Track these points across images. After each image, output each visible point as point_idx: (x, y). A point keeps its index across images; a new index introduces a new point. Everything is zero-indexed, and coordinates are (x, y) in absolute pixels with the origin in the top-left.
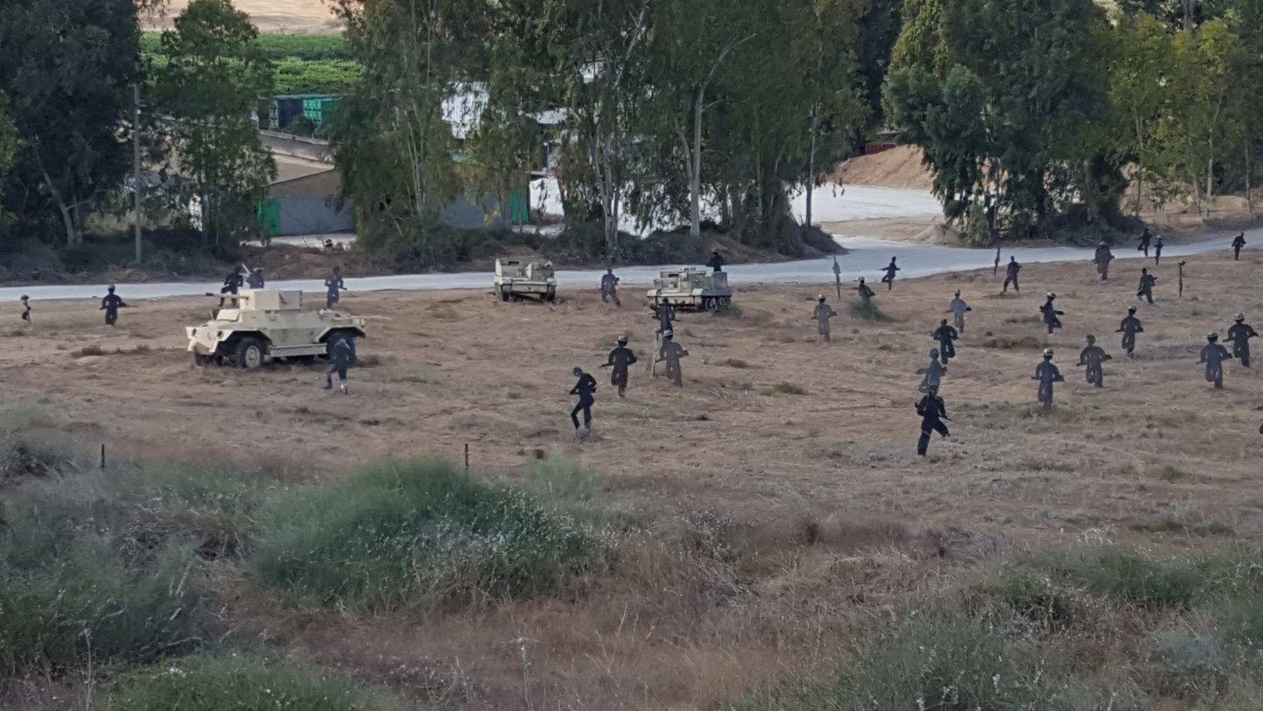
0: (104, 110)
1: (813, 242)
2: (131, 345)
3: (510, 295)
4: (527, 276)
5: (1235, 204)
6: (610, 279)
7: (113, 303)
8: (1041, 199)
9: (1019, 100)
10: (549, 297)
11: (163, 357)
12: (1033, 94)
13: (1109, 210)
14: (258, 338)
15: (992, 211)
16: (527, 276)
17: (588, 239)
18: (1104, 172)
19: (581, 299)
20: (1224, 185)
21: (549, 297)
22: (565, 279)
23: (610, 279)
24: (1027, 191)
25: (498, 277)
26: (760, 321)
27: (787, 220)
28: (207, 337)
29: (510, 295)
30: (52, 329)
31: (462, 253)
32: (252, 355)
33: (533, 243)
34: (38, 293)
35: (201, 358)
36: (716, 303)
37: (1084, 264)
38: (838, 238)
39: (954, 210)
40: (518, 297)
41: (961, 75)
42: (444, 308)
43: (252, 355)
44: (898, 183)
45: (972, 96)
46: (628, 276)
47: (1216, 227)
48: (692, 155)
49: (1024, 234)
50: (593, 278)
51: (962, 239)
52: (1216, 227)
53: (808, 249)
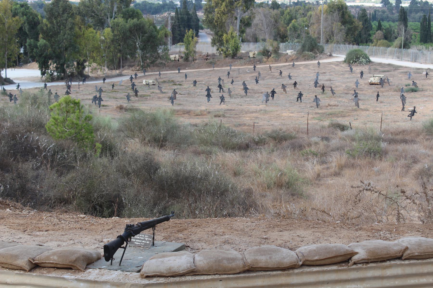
1: (9, 81)
8: (64, 71)
9: (57, 47)
12: (60, 46)
15: (52, 74)
18: (81, 65)
24: (61, 69)
37: (62, 86)
38: (14, 81)
39: (43, 74)
53: (6, 83)
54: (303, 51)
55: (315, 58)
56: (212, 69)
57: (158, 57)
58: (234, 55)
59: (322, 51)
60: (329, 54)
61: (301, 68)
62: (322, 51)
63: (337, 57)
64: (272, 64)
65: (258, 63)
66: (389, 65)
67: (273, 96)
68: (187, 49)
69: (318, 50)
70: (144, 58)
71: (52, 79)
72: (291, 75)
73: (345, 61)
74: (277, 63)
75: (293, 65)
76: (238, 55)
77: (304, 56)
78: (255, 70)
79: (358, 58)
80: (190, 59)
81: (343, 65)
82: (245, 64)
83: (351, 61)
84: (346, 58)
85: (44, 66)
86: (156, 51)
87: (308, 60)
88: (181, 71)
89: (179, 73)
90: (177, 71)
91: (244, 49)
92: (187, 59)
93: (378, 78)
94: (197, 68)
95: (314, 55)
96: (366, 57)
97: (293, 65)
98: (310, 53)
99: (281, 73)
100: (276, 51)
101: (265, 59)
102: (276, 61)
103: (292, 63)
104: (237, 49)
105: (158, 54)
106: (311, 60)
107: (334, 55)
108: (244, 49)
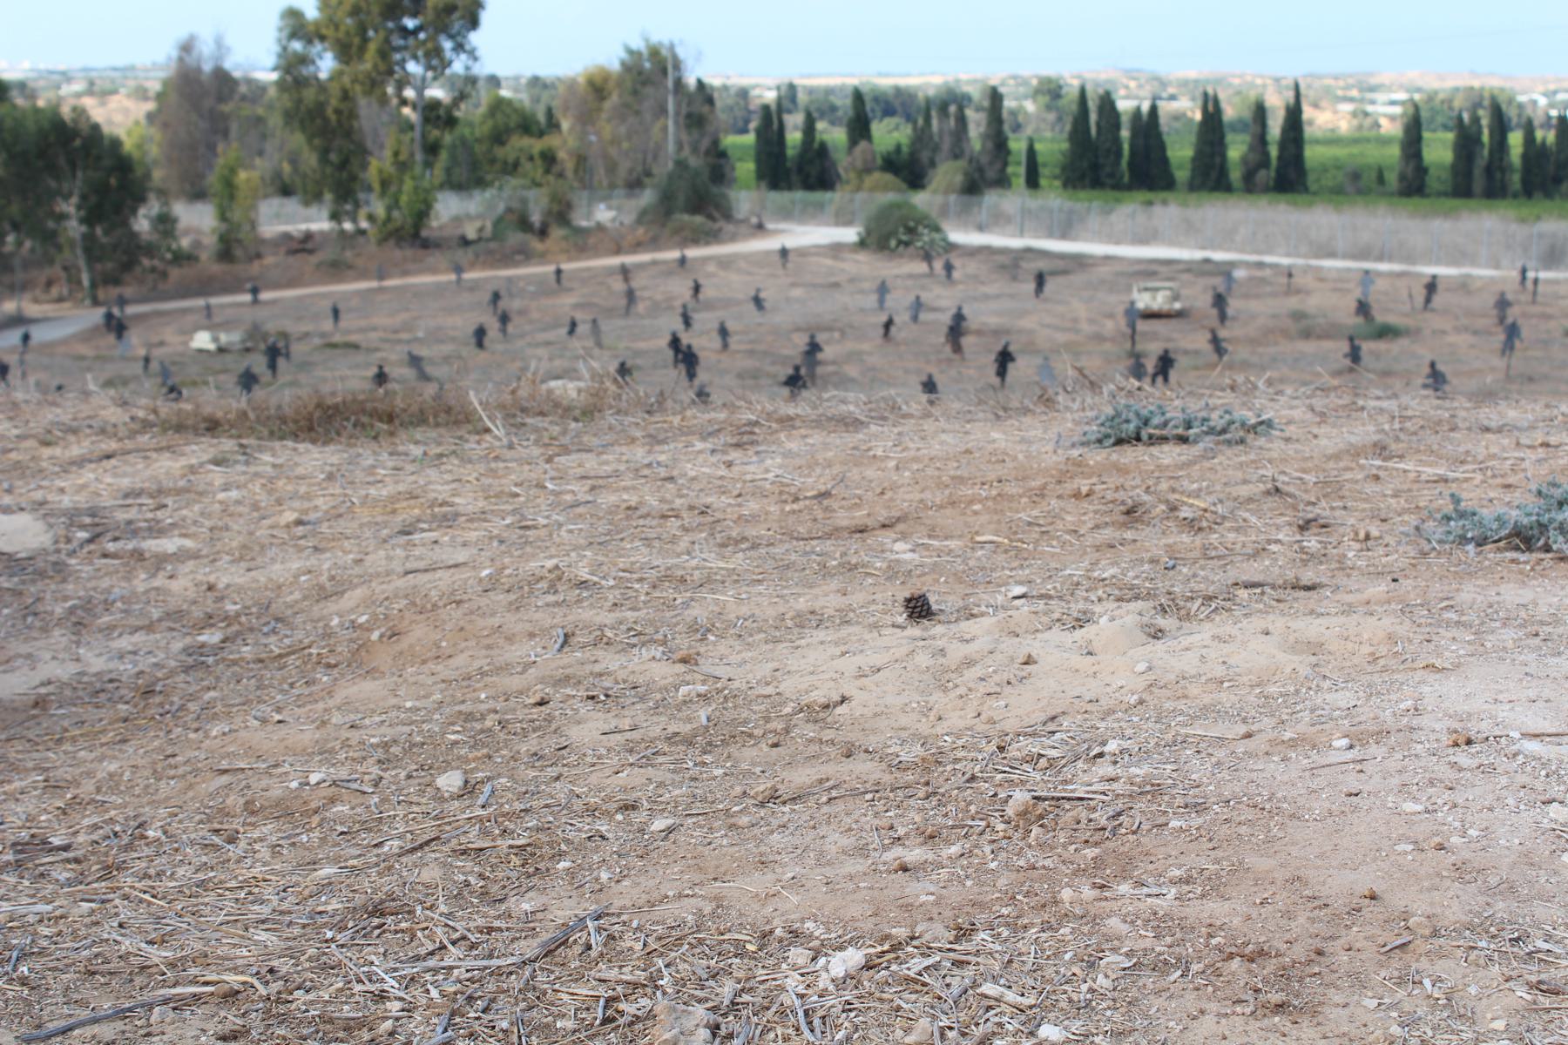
55: (712, 237)
56: (374, 284)
58: (412, 235)
59: (728, 216)
60: (754, 220)
61: (711, 268)
62: (728, 216)
63: (782, 231)
64: (570, 260)
65: (518, 257)
66: (1029, 250)
68: (223, 217)
69: (718, 207)
70: (91, 249)
72: (762, 295)
73: (862, 244)
74: (588, 258)
75: (683, 261)
76: (424, 233)
77: (677, 231)
78: (558, 281)
79: (911, 231)
80: (238, 252)
81: (862, 257)
82: (473, 266)
83: (893, 243)
84: (869, 232)
86: (125, 224)
88: (265, 296)
89: (255, 301)
90: (247, 298)
93: (1168, 293)
94: (291, 284)
95: (710, 224)
96: (937, 229)
97: (683, 261)
98: (698, 219)
99: (697, 288)
100: (561, 214)
101: (536, 244)
103: (674, 254)
104: (422, 214)
105: (134, 236)
106: (707, 243)
107: (770, 226)
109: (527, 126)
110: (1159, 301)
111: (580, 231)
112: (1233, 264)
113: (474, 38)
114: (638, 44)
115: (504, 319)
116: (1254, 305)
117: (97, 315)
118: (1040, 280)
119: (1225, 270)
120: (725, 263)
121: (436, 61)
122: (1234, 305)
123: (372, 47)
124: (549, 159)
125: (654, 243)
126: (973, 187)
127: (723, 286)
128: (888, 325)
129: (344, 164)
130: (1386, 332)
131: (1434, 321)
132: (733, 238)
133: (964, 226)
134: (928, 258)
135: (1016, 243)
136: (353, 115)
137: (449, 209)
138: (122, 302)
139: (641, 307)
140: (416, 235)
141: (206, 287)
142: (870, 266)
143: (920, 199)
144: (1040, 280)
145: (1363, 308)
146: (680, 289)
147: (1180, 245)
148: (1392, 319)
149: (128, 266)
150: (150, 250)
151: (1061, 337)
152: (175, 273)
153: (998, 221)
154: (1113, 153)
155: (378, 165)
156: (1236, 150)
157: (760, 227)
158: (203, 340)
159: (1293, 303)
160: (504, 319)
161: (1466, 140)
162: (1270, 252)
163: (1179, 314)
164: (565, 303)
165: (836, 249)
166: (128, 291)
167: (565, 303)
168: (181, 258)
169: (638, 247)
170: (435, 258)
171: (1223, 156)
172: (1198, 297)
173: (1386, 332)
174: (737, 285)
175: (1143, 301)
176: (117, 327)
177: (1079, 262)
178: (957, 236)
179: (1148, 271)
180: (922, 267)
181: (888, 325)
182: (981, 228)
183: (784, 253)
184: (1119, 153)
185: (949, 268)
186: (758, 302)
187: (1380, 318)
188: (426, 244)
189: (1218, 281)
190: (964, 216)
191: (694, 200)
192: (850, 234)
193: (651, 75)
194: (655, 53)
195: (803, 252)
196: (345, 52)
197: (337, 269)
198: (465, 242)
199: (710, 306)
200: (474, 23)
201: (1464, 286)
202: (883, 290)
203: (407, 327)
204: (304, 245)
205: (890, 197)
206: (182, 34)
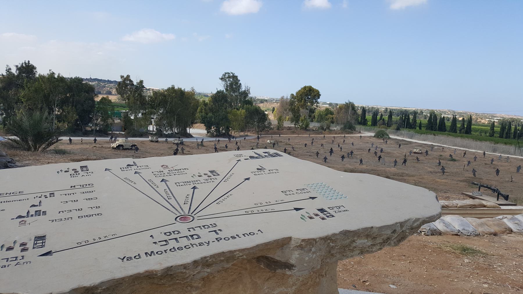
0: (90, 112)
1: (190, 136)
2: (100, 146)
3: (152, 141)
4: (154, 138)
5: (242, 134)
6: (166, 140)
7: (95, 140)
10: (157, 142)
11: (106, 148)
13: (228, 133)
14: (122, 146)
16: (154, 138)
17: (159, 134)
18: (227, 129)
19: (163, 142)
20: (242, 131)
21: (157, 142)
22: (160, 139)
23: (166, 140)
24: (217, 130)
25: (150, 138)
26: (188, 146)
27: (187, 133)
28: (114, 145)
29: (152, 141)
30: (86, 143)
31: (141, 136)
32: (121, 148)
33: (152, 134)
34: (83, 138)
35: (113, 148)
36: (182, 143)
39: (208, 132)
40: (153, 142)
41: (210, 114)
42: (142, 142)
43: (121, 148)
44: (200, 128)
45: (211, 117)
46: (169, 139)
47: (241, 136)
48: (174, 123)
49: (217, 136)
50: (164, 139)
51: (209, 137)
52: (241, 136)
54: (345, 129)
55: (352, 133)
57: (265, 127)
58: (306, 128)
59: (355, 130)
62: (355, 130)
67: (352, 154)
70: (259, 127)
71: (212, 136)
73: (374, 136)
85: (208, 128)
87: (348, 134)
91: (312, 125)
92: (278, 129)
102: (330, 133)
104: (307, 126)
105: (265, 125)
108: (312, 125)
109: (332, 113)
110: (417, 151)
111: (332, 130)
112: (435, 146)
113: (319, 100)
114: (347, 102)
115: (312, 143)
116: (435, 153)
117: (256, 136)
118: (400, 145)
119: (432, 147)
120: (352, 137)
121: (312, 103)
122: (429, 153)
123: (303, 101)
124: (332, 118)
125: (342, 133)
126: (398, 129)
127: (349, 141)
128: (369, 150)
129: (297, 117)
130: (454, 160)
131: (464, 159)
132: (355, 134)
133: (395, 135)
134: (384, 140)
135: (401, 138)
136: (299, 110)
137: (313, 125)
138: (261, 135)
139: (335, 143)
140: (306, 129)
141: (275, 133)
142: (375, 140)
143: (388, 131)
144: (400, 145)
145: (451, 156)
146: (342, 140)
147: (431, 141)
148: (457, 158)
149: (263, 130)
150: (267, 127)
151: (398, 155)
152: (270, 131)
153: (401, 135)
154: (436, 124)
155: (302, 118)
156: (459, 125)
157: (360, 132)
158: (268, 141)
159: (442, 154)
160: (312, 143)
161: (503, 128)
162: (445, 144)
163: (421, 153)
164: (323, 142)
165: (371, 136)
166: (262, 133)
167: (323, 142)
168: (271, 129)
169: (339, 133)
170: (308, 132)
171: (456, 127)
172: (424, 151)
173: (454, 160)
174: (352, 140)
175: (415, 150)
176: (258, 138)
177: (410, 142)
178: (391, 136)
179: (421, 145)
180: (383, 141)
181: (369, 150)
182: (398, 136)
183: (361, 136)
184: (436, 125)
185: (386, 142)
186: (353, 144)
187: (454, 158)
188: (309, 130)
189: (428, 149)
190: (394, 134)
191: (349, 128)
192: (373, 134)
193: (350, 107)
194: (350, 103)
195: (365, 137)
196: (299, 101)
197: (293, 133)
198: (313, 130)
199: (346, 144)
200: (319, 98)
201: (474, 153)
202: (373, 144)
203: (299, 142)
204: (289, 128)
205: (383, 129)
206: (282, 96)
